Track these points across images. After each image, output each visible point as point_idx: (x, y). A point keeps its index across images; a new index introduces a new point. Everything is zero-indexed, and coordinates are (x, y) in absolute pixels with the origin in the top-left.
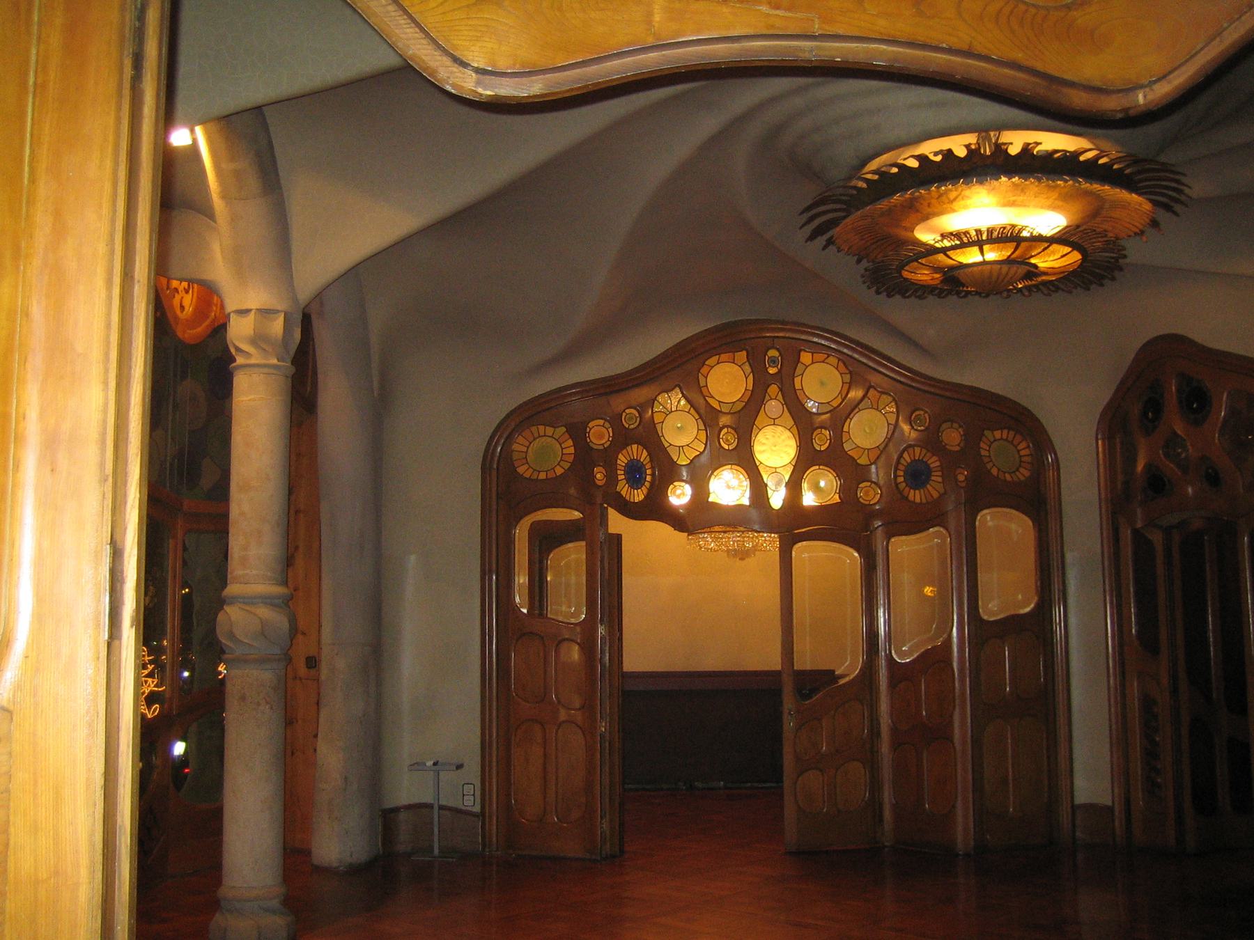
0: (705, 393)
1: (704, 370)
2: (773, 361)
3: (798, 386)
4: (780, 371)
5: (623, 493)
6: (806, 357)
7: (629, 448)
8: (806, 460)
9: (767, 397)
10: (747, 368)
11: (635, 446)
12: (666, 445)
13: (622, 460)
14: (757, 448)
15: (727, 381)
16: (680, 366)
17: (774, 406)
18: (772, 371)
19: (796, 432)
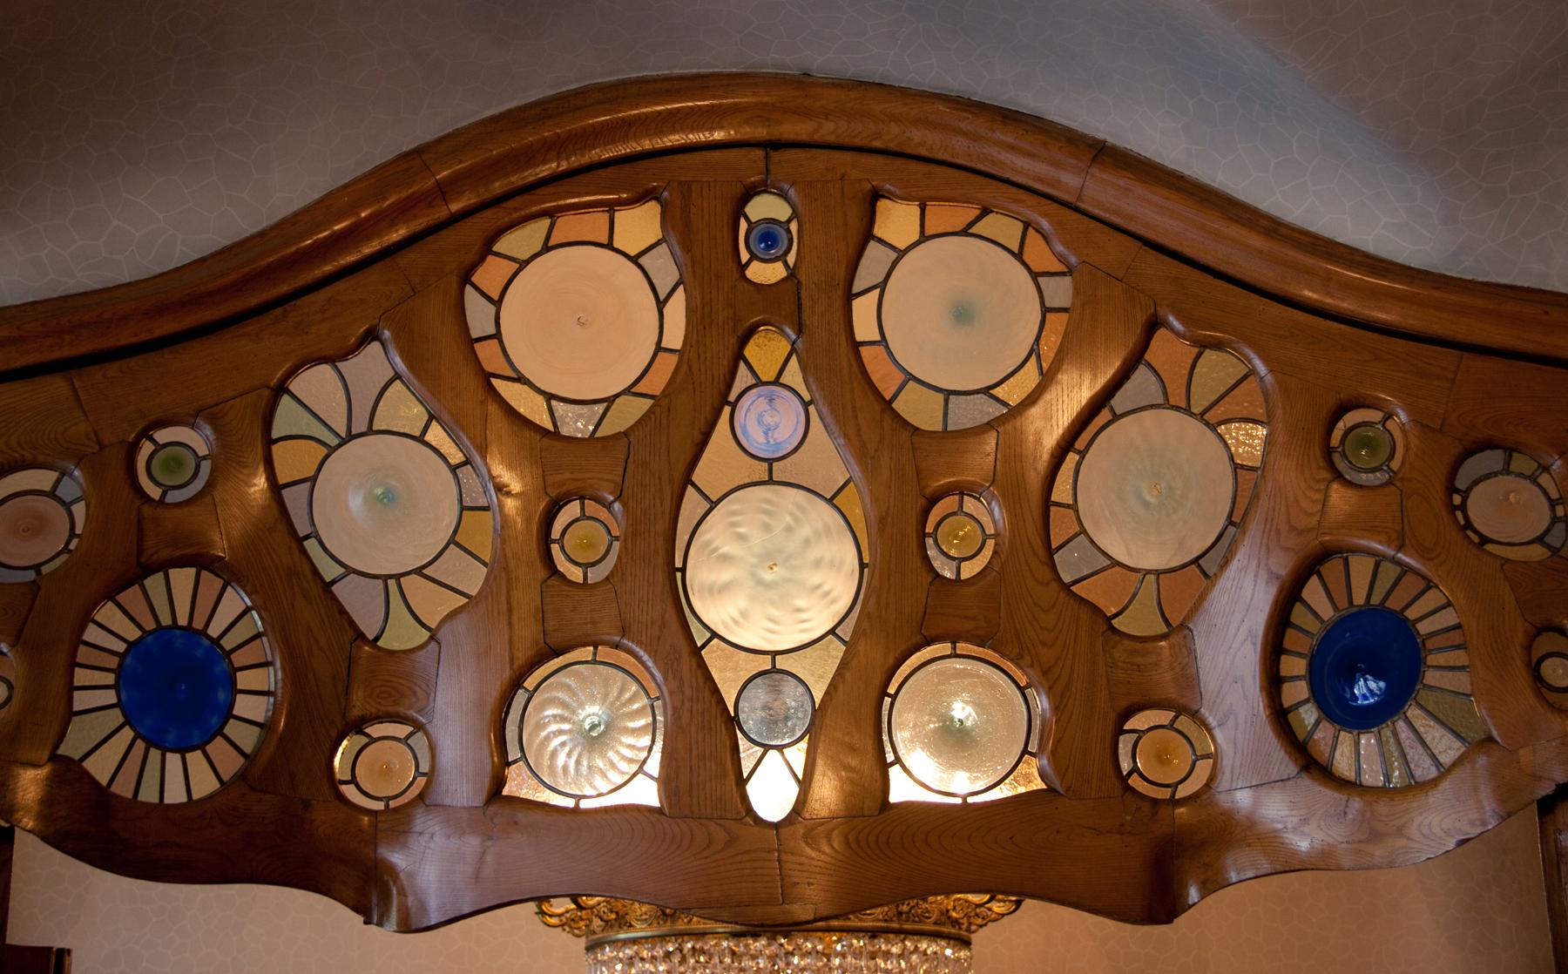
0: (488, 354)
1: (490, 274)
2: (769, 238)
3: (864, 328)
4: (792, 274)
5: (100, 768)
6: (897, 221)
7: (154, 583)
8: (904, 615)
9: (743, 378)
10: (664, 267)
11: (183, 578)
12: (329, 571)
13: (113, 628)
14: (701, 575)
15: (584, 313)
16: (398, 260)
17: (769, 418)
18: (766, 273)
19: (857, 514)
